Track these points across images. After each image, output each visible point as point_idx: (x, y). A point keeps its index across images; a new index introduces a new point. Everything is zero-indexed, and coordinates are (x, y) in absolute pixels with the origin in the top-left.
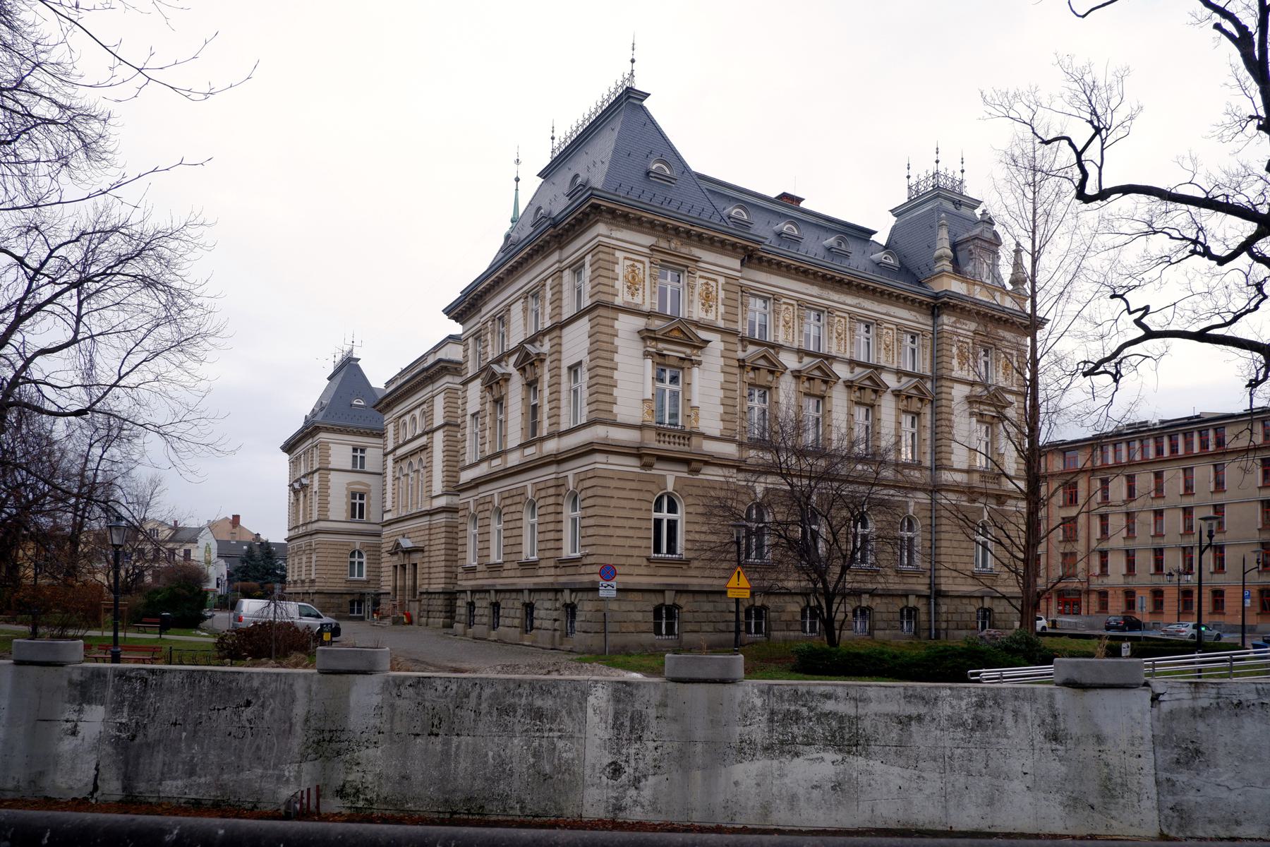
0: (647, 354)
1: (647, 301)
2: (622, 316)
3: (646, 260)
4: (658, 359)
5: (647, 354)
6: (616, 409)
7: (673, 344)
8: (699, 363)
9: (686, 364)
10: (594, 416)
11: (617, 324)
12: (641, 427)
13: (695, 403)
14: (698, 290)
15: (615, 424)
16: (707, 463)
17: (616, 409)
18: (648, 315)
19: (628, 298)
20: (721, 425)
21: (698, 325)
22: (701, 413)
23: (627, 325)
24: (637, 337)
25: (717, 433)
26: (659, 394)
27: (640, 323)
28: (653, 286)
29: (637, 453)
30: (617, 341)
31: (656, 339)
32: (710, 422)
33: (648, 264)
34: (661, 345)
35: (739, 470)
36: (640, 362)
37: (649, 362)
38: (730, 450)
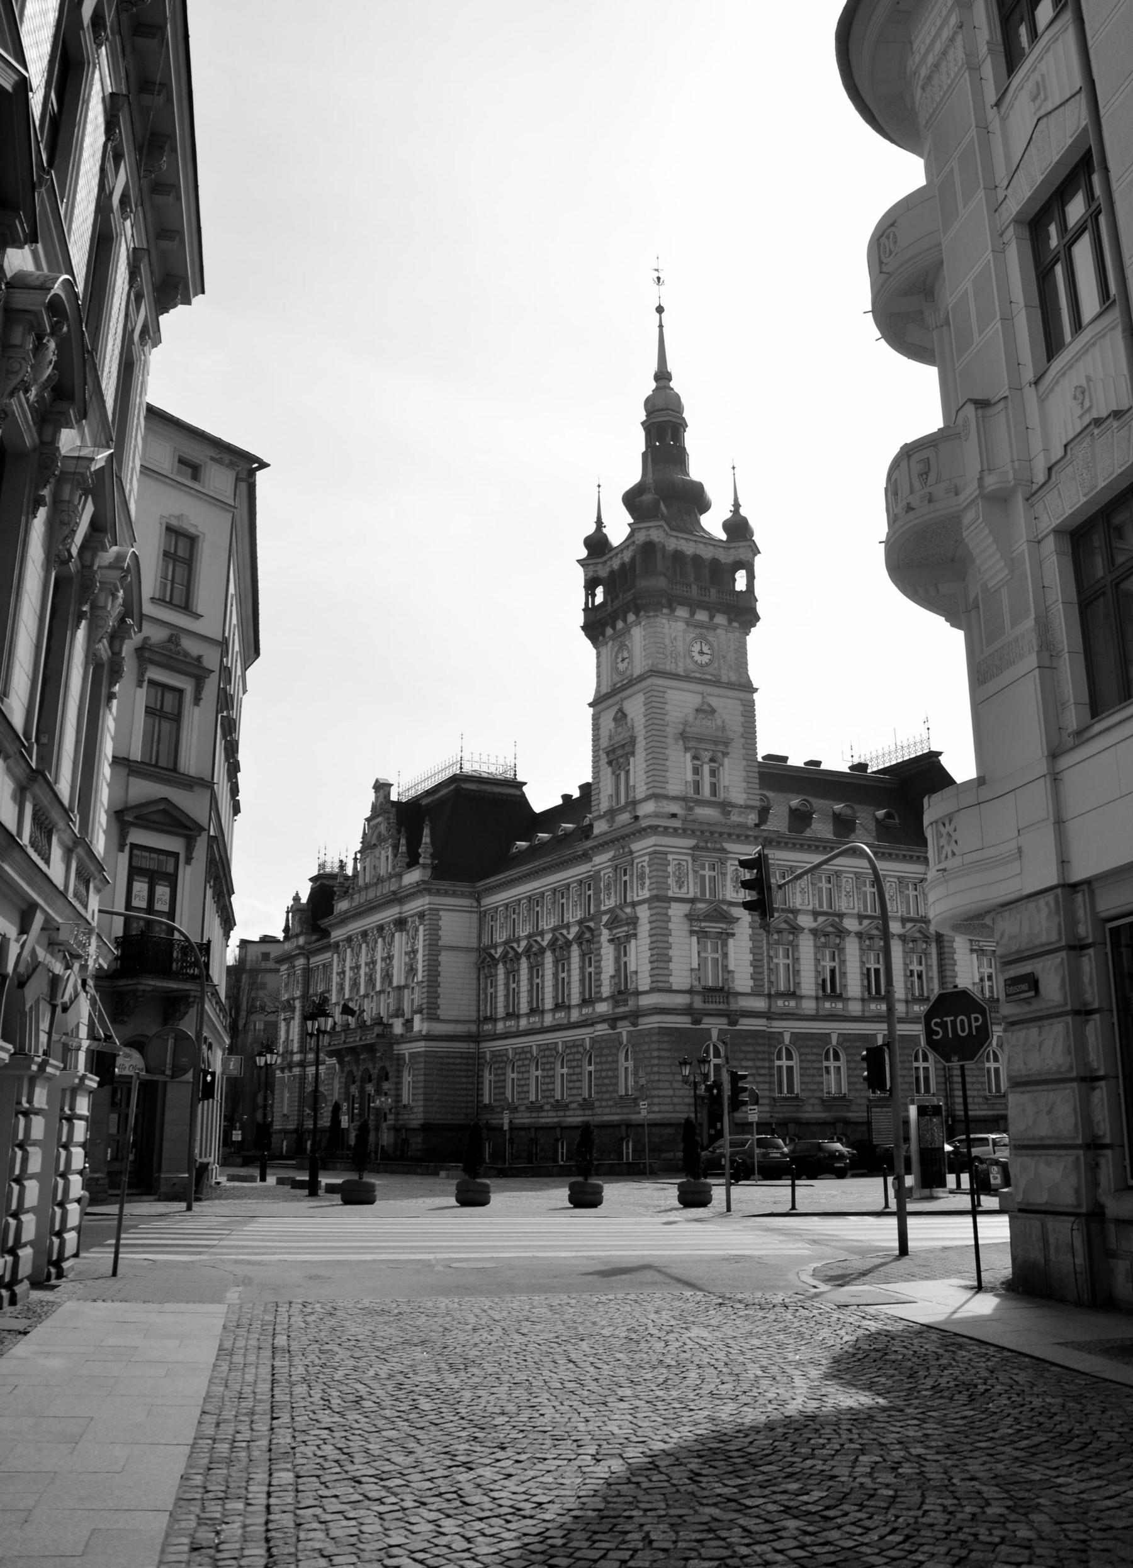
0: (692, 932)
1: (692, 891)
2: (674, 905)
3: (689, 858)
4: (701, 935)
5: (692, 932)
6: (672, 979)
7: (711, 922)
8: (733, 935)
9: (724, 936)
10: (654, 985)
11: (670, 912)
12: (690, 992)
13: (731, 967)
14: (729, 877)
15: (670, 991)
16: (743, 1016)
17: (672, 979)
18: (692, 901)
19: (677, 890)
20: (751, 983)
21: (732, 904)
22: (736, 976)
23: (677, 911)
24: (685, 921)
25: (749, 990)
26: (702, 961)
27: (685, 908)
28: (695, 877)
29: (688, 1010)
30: (671, 926)
31: (701, 921)
32: (743, 981)
33: (690, 862)
34: (703, 924)
35: (769, 1018)
36: (687, 940)
37: (694, 939)
38: (760, 1004)
